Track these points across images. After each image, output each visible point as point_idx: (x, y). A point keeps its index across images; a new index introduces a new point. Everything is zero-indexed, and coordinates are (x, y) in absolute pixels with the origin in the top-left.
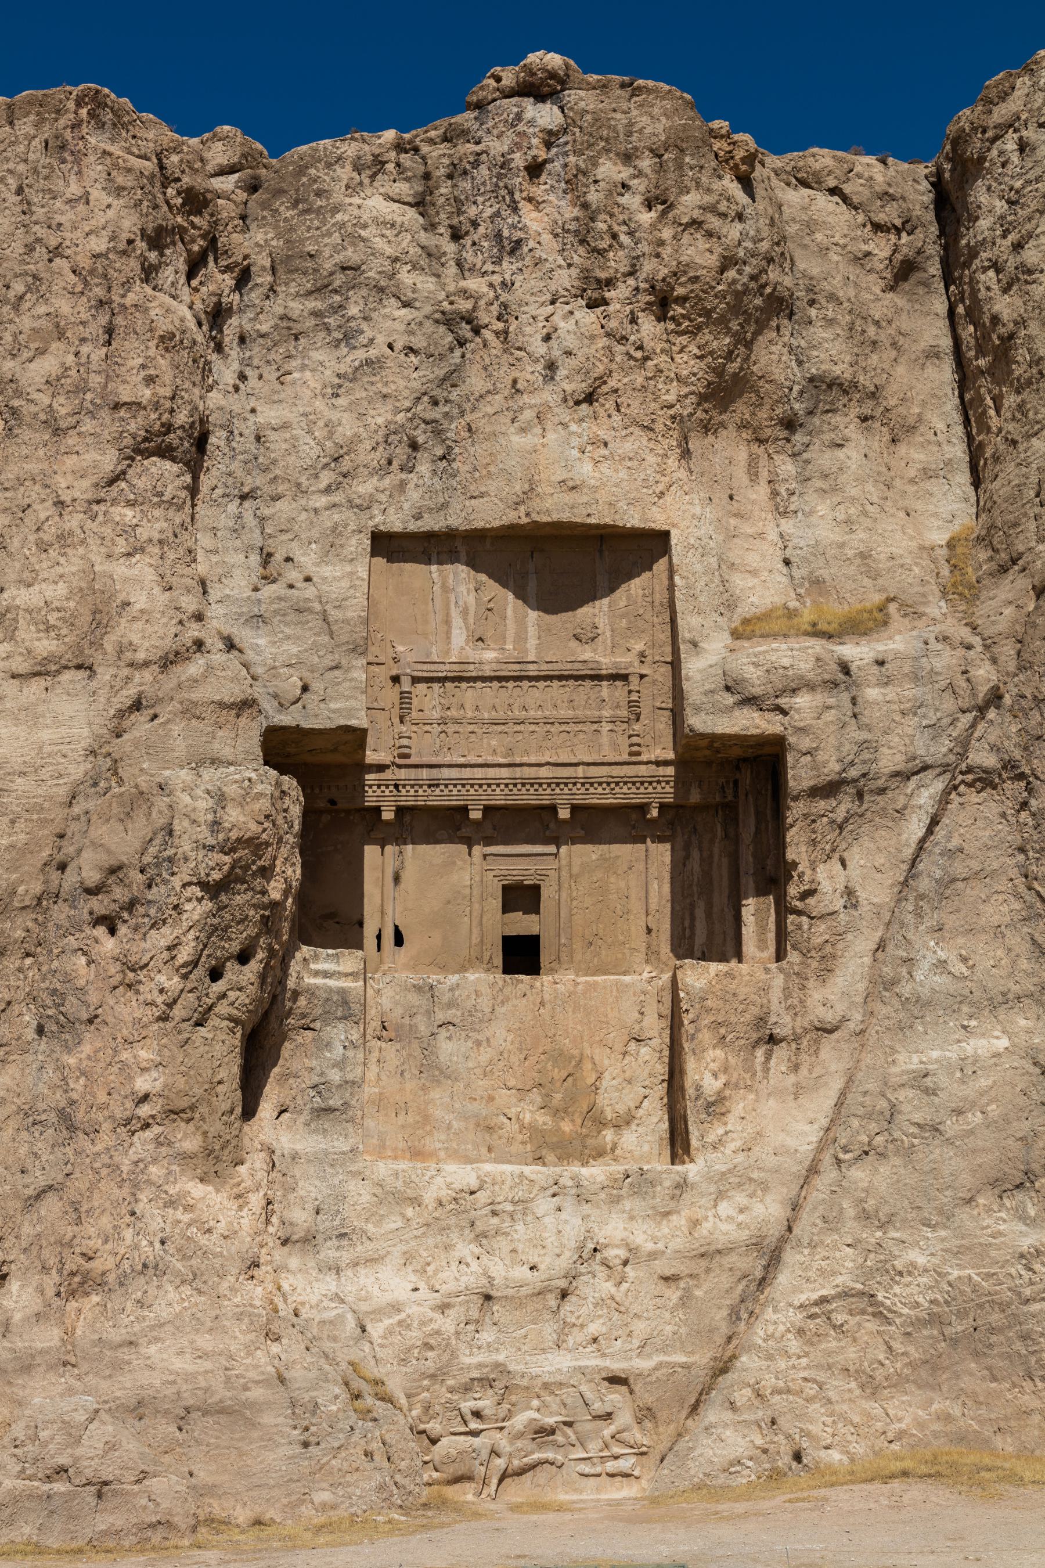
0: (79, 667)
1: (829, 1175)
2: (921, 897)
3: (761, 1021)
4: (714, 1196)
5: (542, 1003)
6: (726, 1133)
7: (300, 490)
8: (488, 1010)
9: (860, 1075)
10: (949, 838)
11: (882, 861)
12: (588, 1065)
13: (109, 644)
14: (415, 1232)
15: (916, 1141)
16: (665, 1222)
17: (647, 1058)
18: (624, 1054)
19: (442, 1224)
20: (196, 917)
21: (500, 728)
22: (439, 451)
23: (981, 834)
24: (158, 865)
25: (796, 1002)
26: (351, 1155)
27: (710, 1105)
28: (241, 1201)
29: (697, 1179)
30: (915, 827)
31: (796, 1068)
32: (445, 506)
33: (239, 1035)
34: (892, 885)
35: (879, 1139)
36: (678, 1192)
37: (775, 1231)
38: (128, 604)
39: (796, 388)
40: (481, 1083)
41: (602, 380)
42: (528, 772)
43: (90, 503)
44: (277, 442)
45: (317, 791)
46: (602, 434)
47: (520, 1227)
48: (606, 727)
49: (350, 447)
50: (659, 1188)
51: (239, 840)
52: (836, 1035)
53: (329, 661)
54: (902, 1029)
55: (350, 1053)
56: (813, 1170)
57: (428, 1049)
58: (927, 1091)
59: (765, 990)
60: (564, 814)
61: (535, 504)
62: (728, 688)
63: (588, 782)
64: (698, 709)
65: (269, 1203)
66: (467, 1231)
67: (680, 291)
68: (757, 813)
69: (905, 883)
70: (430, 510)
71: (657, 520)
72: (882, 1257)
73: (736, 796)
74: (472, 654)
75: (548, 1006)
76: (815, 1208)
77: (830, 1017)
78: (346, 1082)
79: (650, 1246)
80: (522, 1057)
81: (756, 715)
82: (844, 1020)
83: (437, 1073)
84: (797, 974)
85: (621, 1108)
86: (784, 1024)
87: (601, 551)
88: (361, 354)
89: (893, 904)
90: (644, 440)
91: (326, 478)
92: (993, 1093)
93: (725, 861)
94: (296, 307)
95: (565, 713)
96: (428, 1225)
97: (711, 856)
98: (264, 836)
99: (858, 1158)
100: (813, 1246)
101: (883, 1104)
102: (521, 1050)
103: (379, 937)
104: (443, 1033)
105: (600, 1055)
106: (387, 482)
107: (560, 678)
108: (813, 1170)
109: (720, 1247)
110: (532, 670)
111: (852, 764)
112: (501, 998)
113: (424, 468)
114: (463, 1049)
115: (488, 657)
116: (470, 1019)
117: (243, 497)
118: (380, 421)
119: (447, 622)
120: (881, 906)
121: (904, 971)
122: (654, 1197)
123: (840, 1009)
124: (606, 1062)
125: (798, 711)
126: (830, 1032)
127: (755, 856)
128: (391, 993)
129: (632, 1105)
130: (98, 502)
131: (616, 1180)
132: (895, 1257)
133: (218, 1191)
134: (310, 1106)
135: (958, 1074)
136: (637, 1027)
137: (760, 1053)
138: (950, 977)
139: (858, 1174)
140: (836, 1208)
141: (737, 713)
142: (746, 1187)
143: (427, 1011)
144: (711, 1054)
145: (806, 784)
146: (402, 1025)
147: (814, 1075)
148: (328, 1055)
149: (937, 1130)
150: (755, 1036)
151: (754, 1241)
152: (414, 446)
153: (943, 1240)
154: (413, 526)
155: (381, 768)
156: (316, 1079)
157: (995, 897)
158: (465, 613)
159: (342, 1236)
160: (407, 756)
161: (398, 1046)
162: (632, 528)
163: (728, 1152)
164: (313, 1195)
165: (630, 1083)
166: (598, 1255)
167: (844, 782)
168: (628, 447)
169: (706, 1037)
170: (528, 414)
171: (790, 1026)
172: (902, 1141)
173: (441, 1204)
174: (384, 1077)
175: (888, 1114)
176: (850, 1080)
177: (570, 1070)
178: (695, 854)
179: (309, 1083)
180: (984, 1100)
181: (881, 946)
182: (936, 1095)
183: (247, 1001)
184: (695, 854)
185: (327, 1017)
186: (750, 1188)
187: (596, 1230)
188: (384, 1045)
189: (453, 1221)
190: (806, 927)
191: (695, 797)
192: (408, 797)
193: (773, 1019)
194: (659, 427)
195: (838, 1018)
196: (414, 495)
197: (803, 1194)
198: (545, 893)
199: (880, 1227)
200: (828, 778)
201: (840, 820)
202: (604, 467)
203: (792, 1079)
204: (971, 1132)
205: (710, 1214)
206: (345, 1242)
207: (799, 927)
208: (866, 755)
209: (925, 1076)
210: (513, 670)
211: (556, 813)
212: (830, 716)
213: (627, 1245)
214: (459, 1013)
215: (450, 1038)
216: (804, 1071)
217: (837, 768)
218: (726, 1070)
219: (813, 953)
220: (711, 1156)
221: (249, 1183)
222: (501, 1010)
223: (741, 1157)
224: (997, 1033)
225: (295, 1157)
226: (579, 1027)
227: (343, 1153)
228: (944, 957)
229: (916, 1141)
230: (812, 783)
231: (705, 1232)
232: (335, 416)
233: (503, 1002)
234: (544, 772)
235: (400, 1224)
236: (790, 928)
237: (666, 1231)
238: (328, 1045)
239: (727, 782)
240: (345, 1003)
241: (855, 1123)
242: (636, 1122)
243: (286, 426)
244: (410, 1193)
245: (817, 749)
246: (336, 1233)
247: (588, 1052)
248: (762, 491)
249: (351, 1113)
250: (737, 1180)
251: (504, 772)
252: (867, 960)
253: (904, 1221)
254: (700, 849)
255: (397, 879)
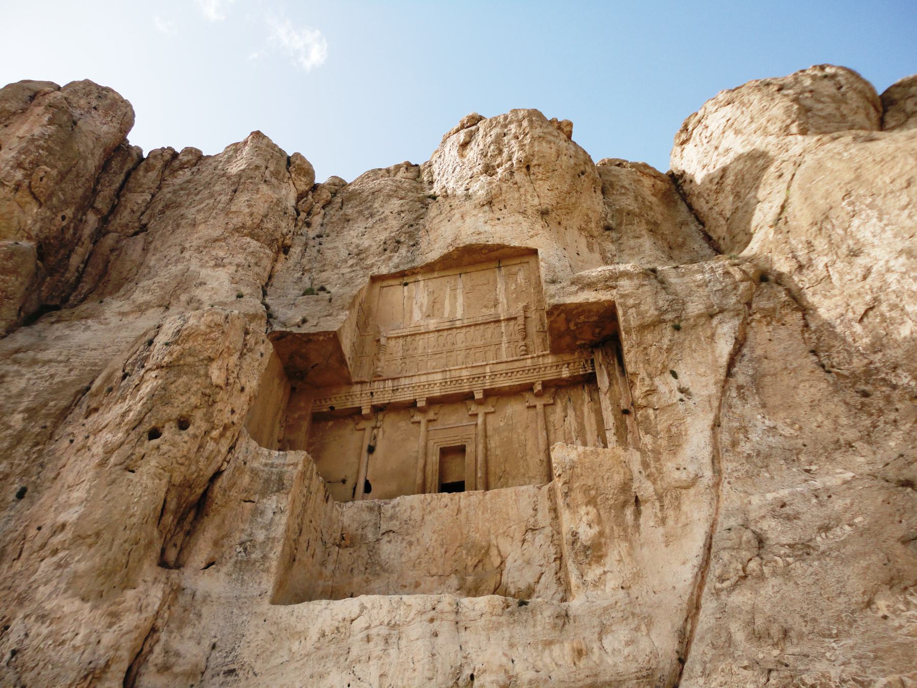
0: (160, 306)
1: (708, 606)
2: (740, 388)
3: (625, 487)
4: (598, 629)
5: (459, 511)
6: (605, 573)
7: (336, 267)
8: (419, 519)
9: (720, 519)
10: (753, 351)
11: (703, 370)
12: (494, 552)
13: (184, 297)
14: (298, 665)
15: (790, 560)
16: (547, 652)
17: (542, 542)
18: (524, 541)
19: (322, 653)
20: (148, 389)
21: (438, 356)
22: (411, 243)
23: (777, 348)
24: (133, 364)
25: (654, 470)
26: (259, 599)
27: (587, 548)
28: (114, 620)
29: (580, 612)
30: (724, 347)
31: (663, 521)
32: (413, 261)
33: (165, 481)
34: (716, 383)
35: (753, 565)
36: (560, 622)
37: (667, 664)
38: (205, 284)
39: (609, 216)
40: (411, 573)
41: (496, 196)
42: (454, 374)
43: (199, 247)
44: (329, 254)
45: (324, 403)
46: (497, 216)
47: (393, 652)
48: (504, 346)
49: (367, 249)
50: (539, 617)
51: (189, 335)
52: (692, 491)
53: (325, 313)
54: (750, 477)
55: (277, 517)
56: (695, 607)
57: (373, 550)
58: (788, 518)
59: (626, 464)
60: (478, 396)
61: (458, 242)
62: (573, 283)
63: (494, 375)
64: (552, 296)
65: (154, 630)
66: (342, 659)
67: (535, 162)
68: (609, 375)
69: (726, 381)
70: (403, 264)
71: (531, 244)
72: (787, 673)
73: (593, 369)
74: (422, 323)
75: (464, 511)
76: (702, 638)
77: (683, 476)
78: (268, 538)
79: (531, 674)
80: (443, 550)
81: (594, 294)
82: (697, 477)
83: (378, 568)
84: (652, 451)
85: (522, 585)
86: (645, 489)
87: (499, 267)
88: (377, 218)
89: (719, 394)
90: (521, 217)
91: (350, 262)
92: (855, 508)
93: (593, 416)
94: (349, 211)
95: (479, 343)
96: (308, 655)
97: (582, 413)
98: (212, 335)
99: (735, 586)
100: (706, 674)
101: (747, 535)
102: (442, 545)
103: (354, 489)
104: (386, 538)
105: (506, 546)
106: (383, 258)
107: (476, 325)
108: (695, 607)
109: (607, 678)
110: (458, 324)
111: (666, 311)
112: (429, 509)
113: (403, 250)
114: (399, 549)
115: (432, 324)
116: (405, 527)
117: (304, 271)
118: (383, 238)
119: (411, 312)
120: (709, 396)
121: (741, 436)
122: (534, 626)
123: (692, 469)
124: (509, 548)
125: (623, 286)
126: (687, 488)
127: (611, 398)
128: (351, 514)
129: (532, 581)
130: (205, 247)
131: (494, 607)
132: (802, 672)
133: (94, 608)
134: (233, 560)
135: (814, 501)
136: (532, 520)
137: (629, 512)
138: (782, 438)
139: (741, 598)
140: (724, 635)
141: (580, 293)
142: (630, 620)
143: (375, 524)
144: (583, 510)
145: (634, 322)
146: (356, 535)
147: (680, 525)
148: (260, 520)
149: (809, 547)
150: (622, 498)
151: (644, 673)
152: (398, 242)
153: (852, 648)
154: (393, 271)
155: (362, 383)
156: (244, 537)
157: (802, 385)
158: (421, 307)
159: (231, 672)
160: (380, 376)
161: (351, 550)
162: (514, 247)
163: (608, 590)
164: (213, 633)
165: (528, 563)
166: (476, 682)
167: (664, 321)
168: (511, 219)
169: (578, 496)
170: (458, 216)
171: (651, 489)
172: (776, 561)
173: (324, 635)
174: (337, 574)
175: (755, 543)
176: (713, 526)
177: (480, 557)
178: (571, 412)
179: (238, 541)
180: (848, 515)
181: (716, 425)
182: (799, 518)
183: (179, 455)
184: (571, 412)
185: (264, 494)
186: (633, 623)
187: (474, 656)
188: (341, 551)
189: (333, 648)
190: (652, 417)
191: (565, 373)
192: (379, 400)
193: (635, 485)
194: (529, 212)
195: (692, 476)
196: (396, 260)
197: (689, 627)
198: (468, 449)
199: (775, 645)
200: (651, 319)
201: (665, 347)
202: (498, 228)
203: (661, 530)
204: (844, 543)
205: (596, 646)
206: (230, 679)
207: (647, 418)
208: (676, 307)
209: (782, 506)
210: (447, 325)
211: (473, 397)
212: (647, 288)
213: (506, 671)
214: (398, 523)
215: (390, 542)
216: (670, 522)
217: (656, 313)
218: (600, 522)
219: (662, 434)
220: (592, 593)
221: (134, 603)
222: (428, 518)
223: (621, 593)
224: (838, 471)
225: (206, 598)
226: (487, 524)
227: (252, 597)
228: (772, 425)
229: (790, 560)
230: (638, 323)
231: (591, 664)
232: (361, 242)
233: (430, 512)
234: (465, 373)
235: (286, 658)
236: (640, 419)
237: (547, 660)
238: (262, 513)
239: (587, 361)
240: (280, 480)
241: (725, 556)
242: (536, 595)
243: (335, 248)
244: (300, 627)
245: (639, 304)
246: (226, 668)
247: (494, 542)
248: (597, 256)
249: (267, 565)
250: (620, 614)
251: (439, 377)
252: (708, 433)
253: (801, 636)
254: (575, 409)
255: (371, 450)
